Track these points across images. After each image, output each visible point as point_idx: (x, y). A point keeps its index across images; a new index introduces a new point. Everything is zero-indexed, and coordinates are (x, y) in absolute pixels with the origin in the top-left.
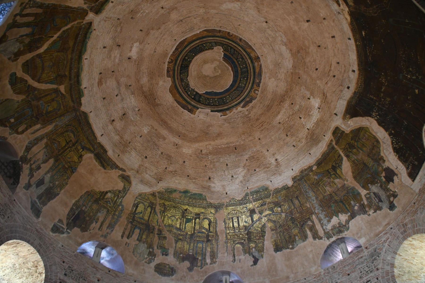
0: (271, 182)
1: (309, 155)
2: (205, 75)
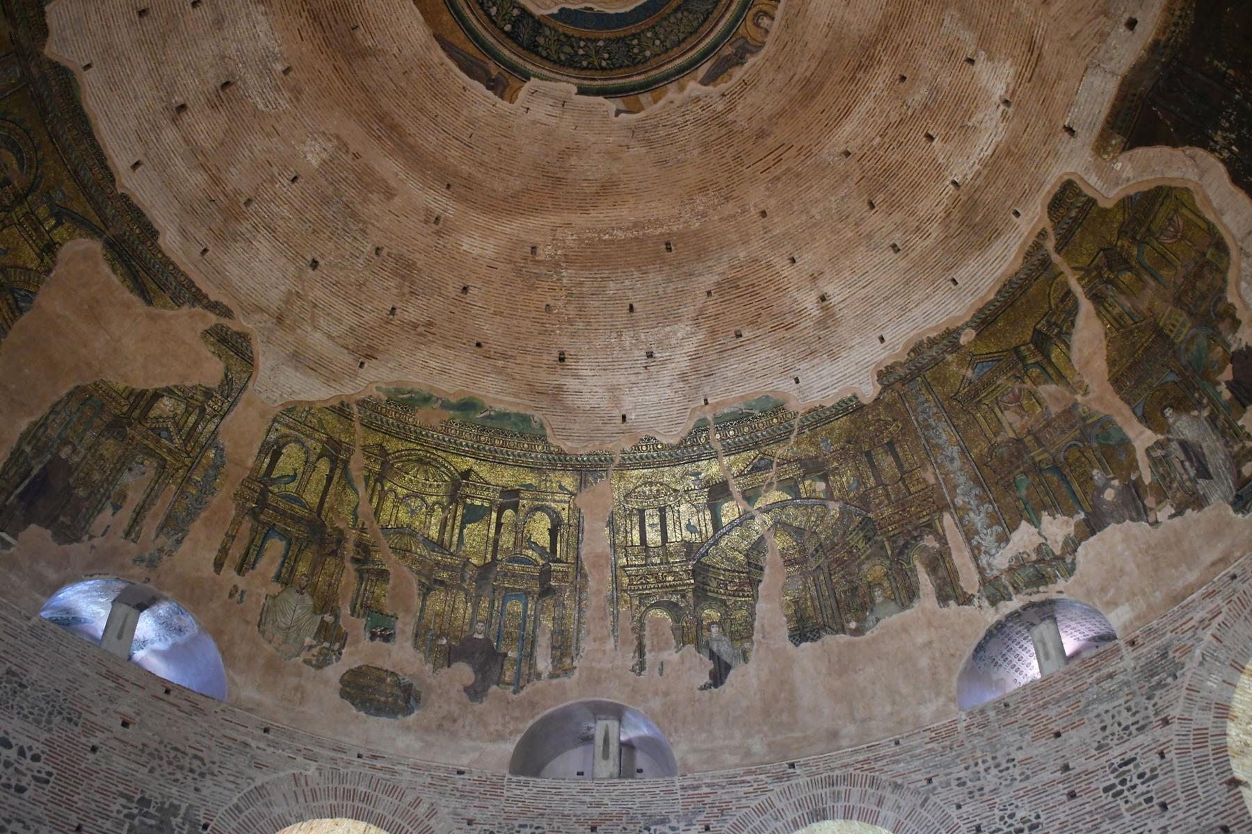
0: (797, 382)
1: (952, 285)
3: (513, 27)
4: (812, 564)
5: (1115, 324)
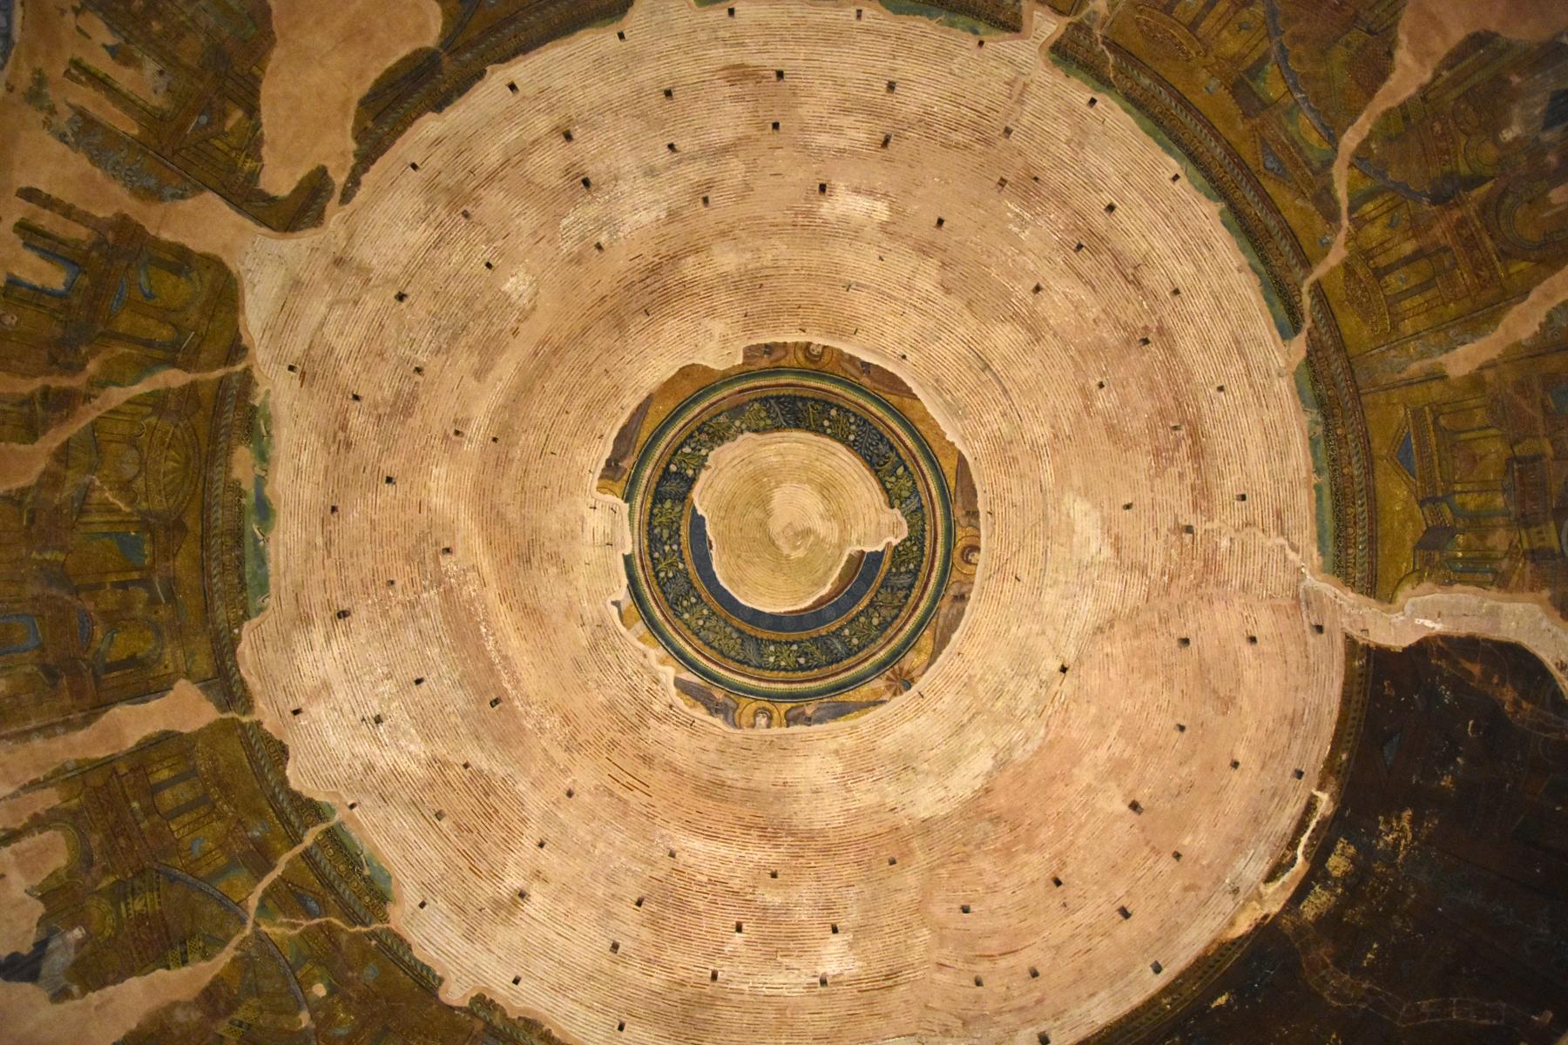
0: (422, 905)
2: (767, 500)
3: (676, 473)
4: (222, 1027)
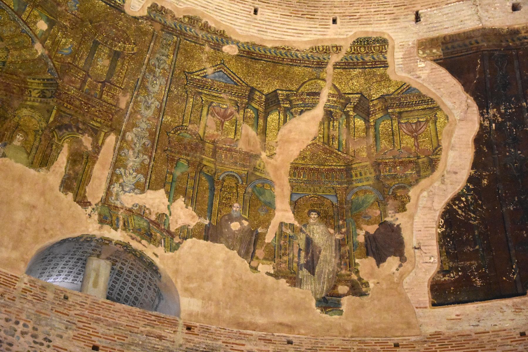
5: (326, 138)
